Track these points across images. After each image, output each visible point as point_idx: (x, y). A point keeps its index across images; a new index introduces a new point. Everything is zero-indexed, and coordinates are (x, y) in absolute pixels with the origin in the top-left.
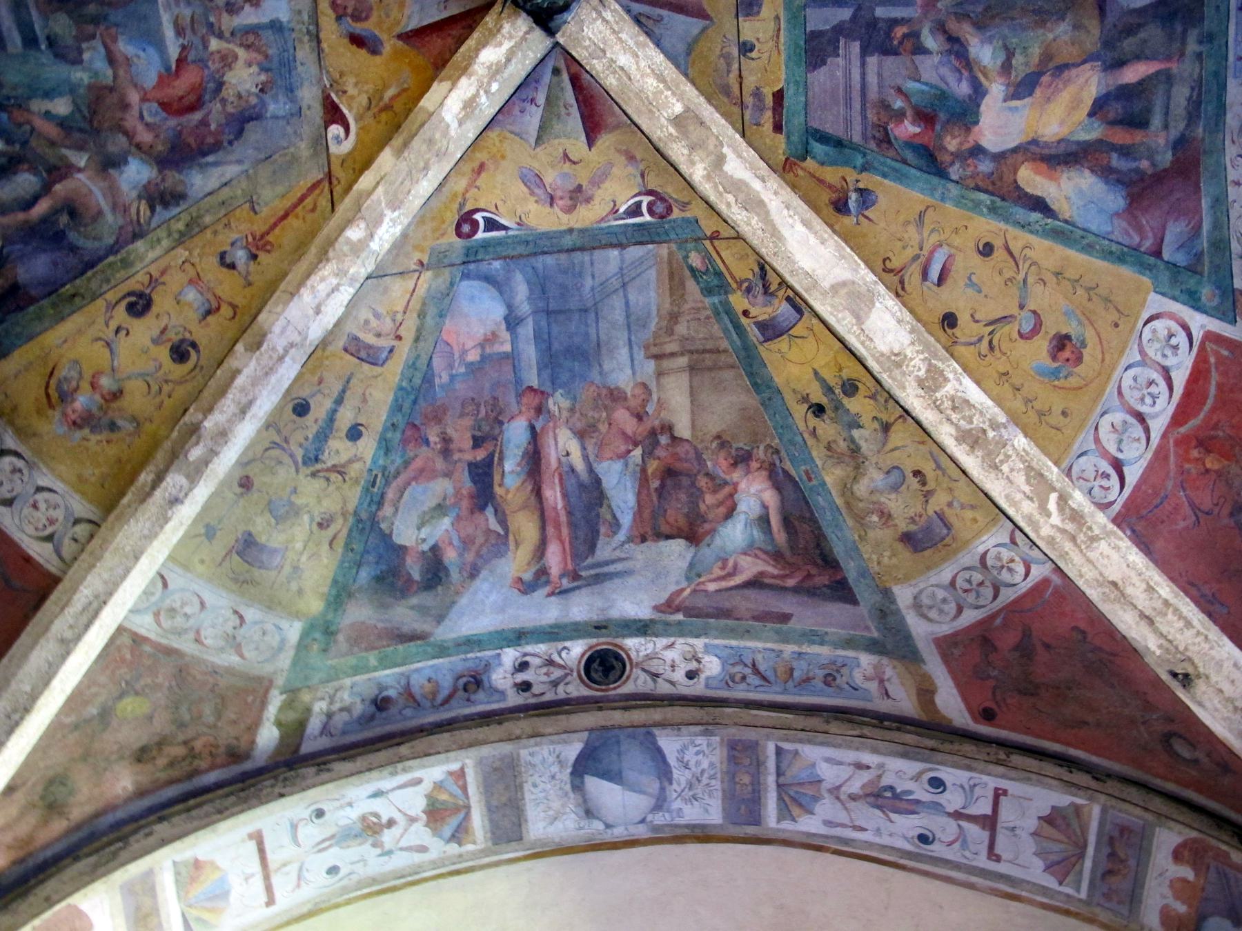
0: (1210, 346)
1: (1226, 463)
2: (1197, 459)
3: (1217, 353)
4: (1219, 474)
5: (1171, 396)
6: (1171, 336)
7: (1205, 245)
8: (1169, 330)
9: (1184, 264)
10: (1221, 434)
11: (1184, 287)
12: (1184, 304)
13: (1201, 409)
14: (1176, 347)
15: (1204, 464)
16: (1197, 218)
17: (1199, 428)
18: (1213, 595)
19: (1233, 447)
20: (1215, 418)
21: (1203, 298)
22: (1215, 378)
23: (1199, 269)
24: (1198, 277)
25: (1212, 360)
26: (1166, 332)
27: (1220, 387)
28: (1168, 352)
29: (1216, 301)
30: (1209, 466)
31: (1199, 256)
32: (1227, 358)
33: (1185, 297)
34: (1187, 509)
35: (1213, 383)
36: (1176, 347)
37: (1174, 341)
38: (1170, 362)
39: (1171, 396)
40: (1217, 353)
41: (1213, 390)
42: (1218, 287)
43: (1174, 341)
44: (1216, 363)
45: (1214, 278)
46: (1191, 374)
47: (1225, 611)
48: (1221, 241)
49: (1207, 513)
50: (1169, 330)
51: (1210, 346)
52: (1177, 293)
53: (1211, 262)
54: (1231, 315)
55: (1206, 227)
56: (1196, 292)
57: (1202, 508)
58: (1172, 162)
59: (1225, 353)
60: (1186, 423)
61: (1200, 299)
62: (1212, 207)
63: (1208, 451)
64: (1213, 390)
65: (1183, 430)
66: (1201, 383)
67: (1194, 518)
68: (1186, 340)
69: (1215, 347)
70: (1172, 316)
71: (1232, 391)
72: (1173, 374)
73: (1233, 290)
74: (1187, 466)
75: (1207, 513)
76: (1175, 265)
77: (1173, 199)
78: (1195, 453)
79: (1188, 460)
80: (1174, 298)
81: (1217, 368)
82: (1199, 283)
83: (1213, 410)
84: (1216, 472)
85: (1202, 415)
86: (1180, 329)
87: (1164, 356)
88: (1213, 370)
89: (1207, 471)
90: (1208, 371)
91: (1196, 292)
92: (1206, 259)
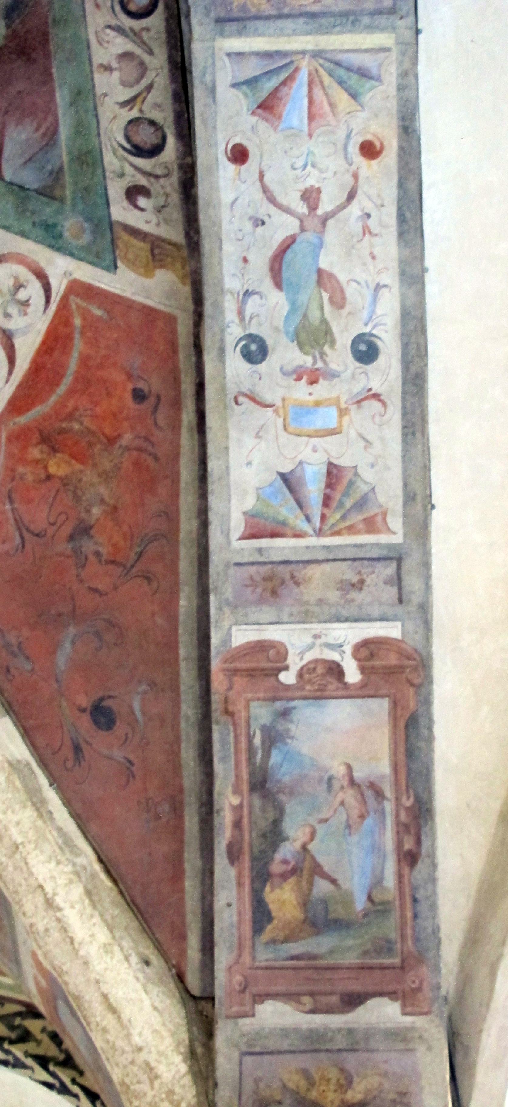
0: (74, 301)
1: (78, 466)
2: (37, 462)
3: (85, 315)
4: (65, 481)
5: (10, 372)
6: (19, 286)
7: (65, 158)
8: (16, 278)
9: (35, 186)
10: (76, 426)
11: (37, 220)
12: (37, 241)
13: (52, 391)
14: (26, 304)
15: (46, 467)
16: (50, 119)
17: (46, 417)
18: (20, 644)
19: (90, 445)
20: (71, 404)
21: (67, 234)
22: (78, 346)
23: (57, 193)
24: (56, 204)
25: (77, 322)
26: (11, 282)
27: (84, 361)
28: (13, 310)
29: (86, 239)
30: (53, 469)
31: (57, 174)
32: (99, 319)
33: (40, 232)
34: (11, 528)
35: (75, 355)
36: (26, 304)
37: (22, 295)
38: (14, 324)
39: (10, 372)
40: (85, 315)
41: (73, 364)
42: (89, 219)
43: (22, 295)
44: (83, 327)
45: (80, 207)
46: (44, 343)
47: (28, 667)
48: (89, 152)
49: (37, 535)
50: (16, 278)
51: (74, 301)
52: (27, 227)
53: (75, 183)
54: (108, 259)
55: (64, 133)
56: (55, 226)
57: (32, 527)
58: (6, 37)
59: (98, 312)
60: (28, 410)
61: (61, 236)
62: (72, 104)
63: (54, 450)
64: (73, 364)
65: (23, 420)
66: (56, 354)
67: (18, 540)
68: (42, 293)
69: (83, 304)
70: (21, 260)
71: (101, 366)
72: (18, 342)
73: (111, 224)
74: (21, 469)
75: (37, 535)
76: (21, 187)
77: (13, 91)
78: (35, 453)
79: (23, 460)
80: (23, 234)
81: (82, 333)
82: (59, 212)
83: (71, 392)
84: (61, 479)
85: (53, 399)
86: (32, 278)
87: (7, 315)
88: (77, 336)
89: (49, 477)
90: (69, 338)
91: (55, 226)
92: (68, 179)
